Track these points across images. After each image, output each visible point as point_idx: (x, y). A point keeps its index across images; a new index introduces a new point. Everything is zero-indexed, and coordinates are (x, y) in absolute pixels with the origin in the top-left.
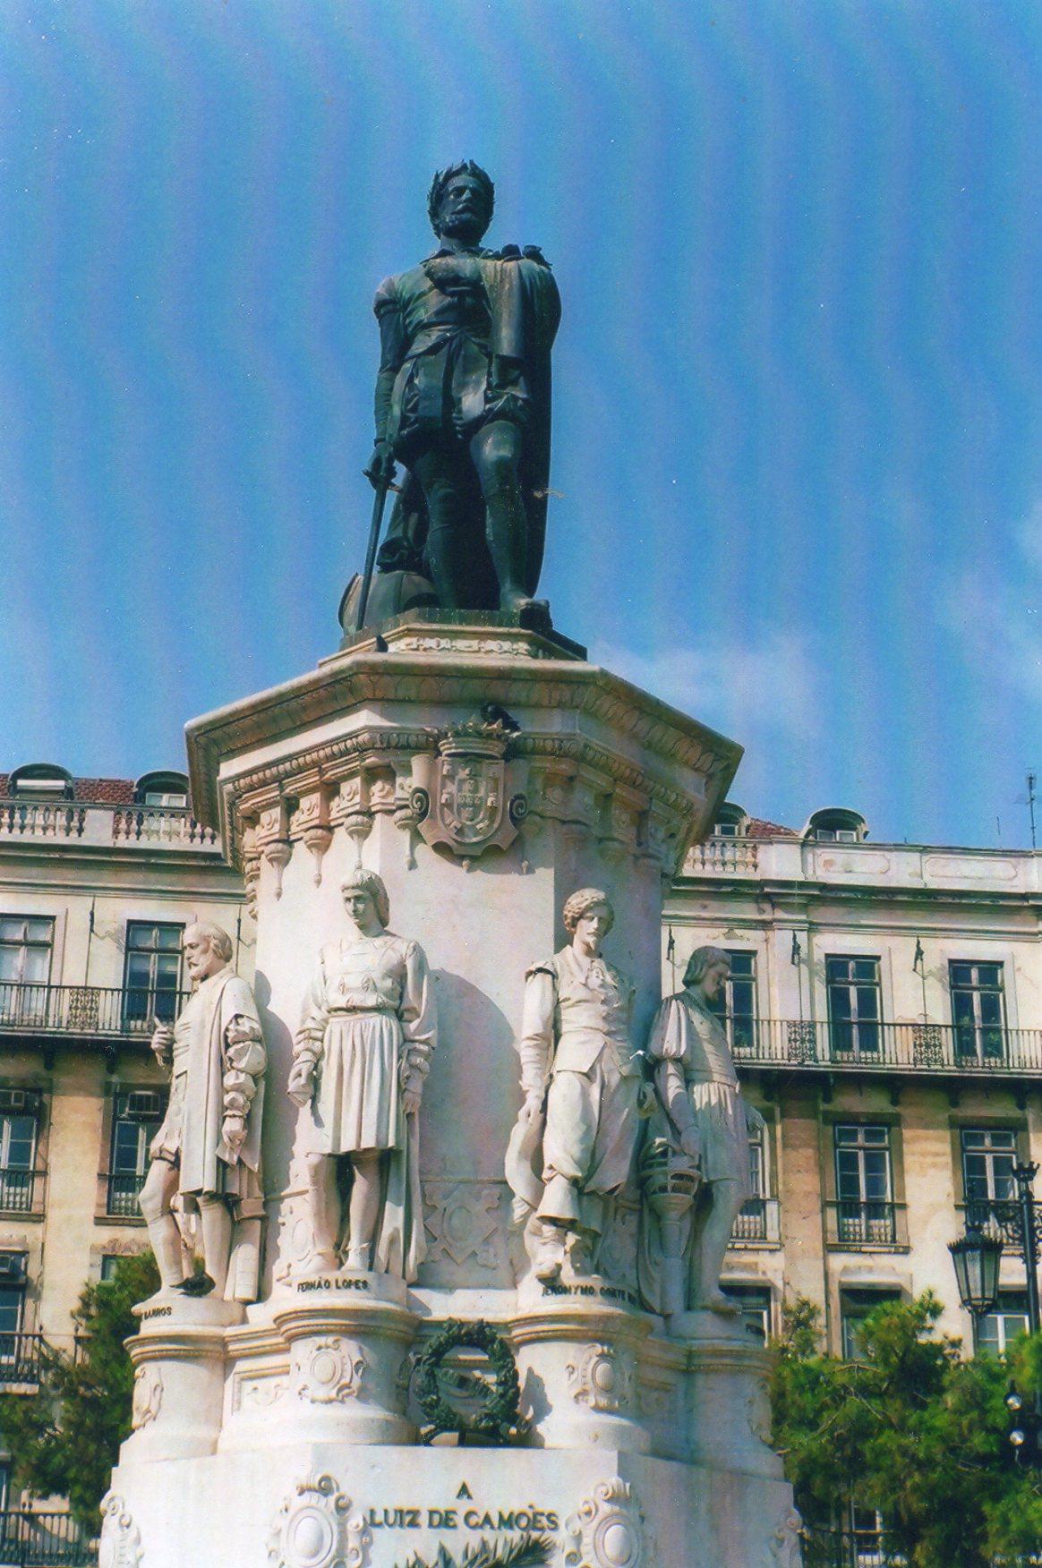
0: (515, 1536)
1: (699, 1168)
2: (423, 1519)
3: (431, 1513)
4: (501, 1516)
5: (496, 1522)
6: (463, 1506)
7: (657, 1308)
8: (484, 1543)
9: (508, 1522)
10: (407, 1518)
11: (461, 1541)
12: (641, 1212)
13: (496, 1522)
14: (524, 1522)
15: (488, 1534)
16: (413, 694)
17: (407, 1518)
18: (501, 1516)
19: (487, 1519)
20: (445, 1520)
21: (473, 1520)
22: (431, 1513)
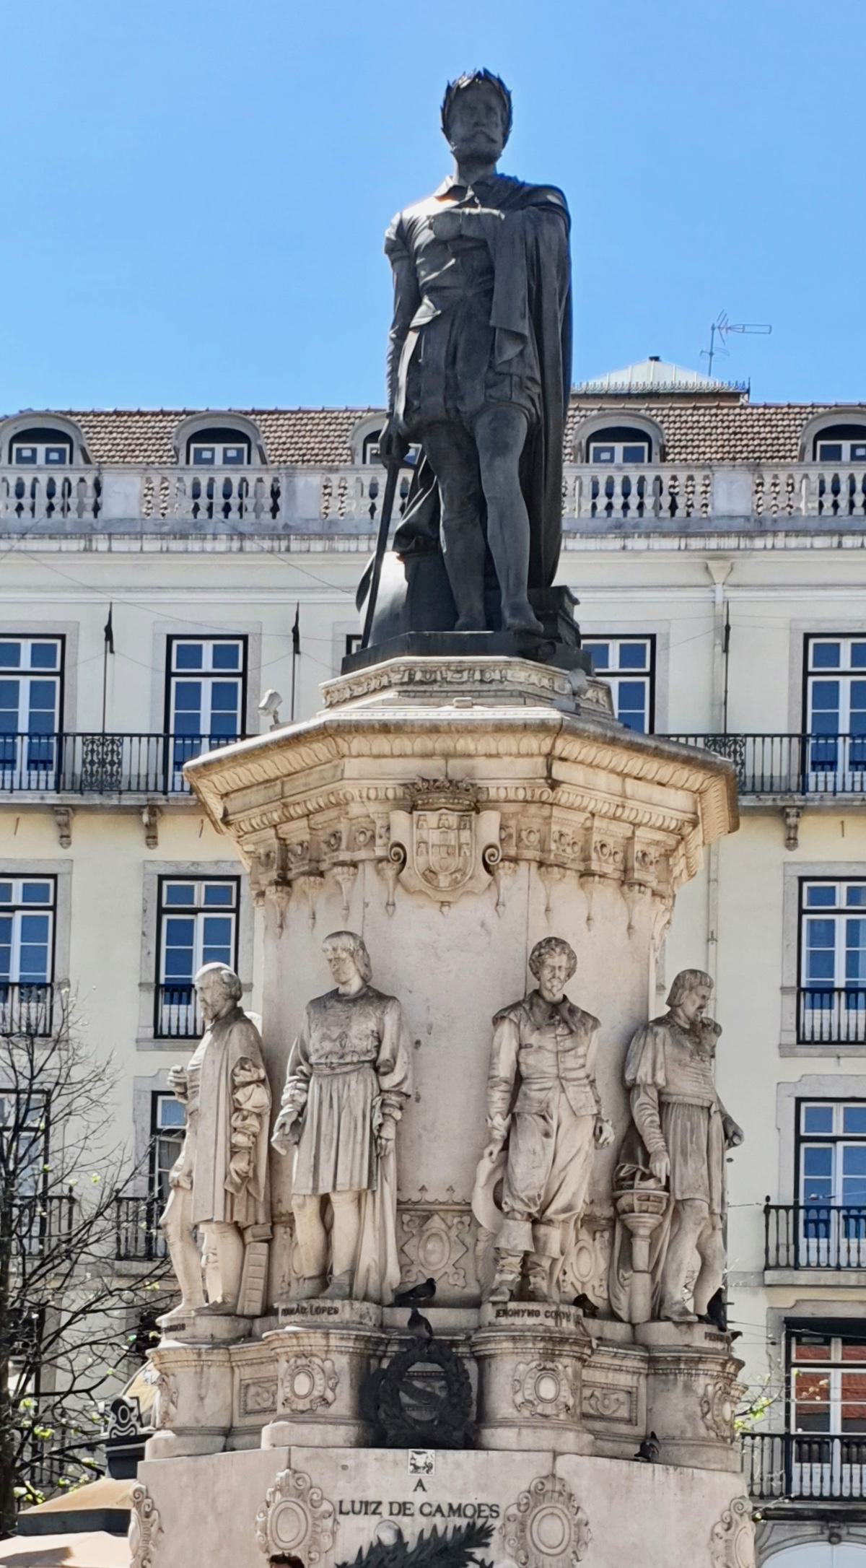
0: (462, 1522)
1: (667, 1188)
2: (384, 1509)
3: (391, 1504)
4: (450, 1506)
5: (445, 1509)
6: (419, 1498)
7: (625, 1317)
8: (435, 1528)
9: (457, 1511)
10: (370, 1508)
11: (413, 1528)
12: (614, 1228)
13: (445, 1509)
14: (469, 1512)
15: (438, 1520)
16: (387, 750)
17: (370, 1508)
18: (450, 1506)
19: (439, 1509)
20: (403, 1508)
21: (427, 1510)
22: (391, 1504)
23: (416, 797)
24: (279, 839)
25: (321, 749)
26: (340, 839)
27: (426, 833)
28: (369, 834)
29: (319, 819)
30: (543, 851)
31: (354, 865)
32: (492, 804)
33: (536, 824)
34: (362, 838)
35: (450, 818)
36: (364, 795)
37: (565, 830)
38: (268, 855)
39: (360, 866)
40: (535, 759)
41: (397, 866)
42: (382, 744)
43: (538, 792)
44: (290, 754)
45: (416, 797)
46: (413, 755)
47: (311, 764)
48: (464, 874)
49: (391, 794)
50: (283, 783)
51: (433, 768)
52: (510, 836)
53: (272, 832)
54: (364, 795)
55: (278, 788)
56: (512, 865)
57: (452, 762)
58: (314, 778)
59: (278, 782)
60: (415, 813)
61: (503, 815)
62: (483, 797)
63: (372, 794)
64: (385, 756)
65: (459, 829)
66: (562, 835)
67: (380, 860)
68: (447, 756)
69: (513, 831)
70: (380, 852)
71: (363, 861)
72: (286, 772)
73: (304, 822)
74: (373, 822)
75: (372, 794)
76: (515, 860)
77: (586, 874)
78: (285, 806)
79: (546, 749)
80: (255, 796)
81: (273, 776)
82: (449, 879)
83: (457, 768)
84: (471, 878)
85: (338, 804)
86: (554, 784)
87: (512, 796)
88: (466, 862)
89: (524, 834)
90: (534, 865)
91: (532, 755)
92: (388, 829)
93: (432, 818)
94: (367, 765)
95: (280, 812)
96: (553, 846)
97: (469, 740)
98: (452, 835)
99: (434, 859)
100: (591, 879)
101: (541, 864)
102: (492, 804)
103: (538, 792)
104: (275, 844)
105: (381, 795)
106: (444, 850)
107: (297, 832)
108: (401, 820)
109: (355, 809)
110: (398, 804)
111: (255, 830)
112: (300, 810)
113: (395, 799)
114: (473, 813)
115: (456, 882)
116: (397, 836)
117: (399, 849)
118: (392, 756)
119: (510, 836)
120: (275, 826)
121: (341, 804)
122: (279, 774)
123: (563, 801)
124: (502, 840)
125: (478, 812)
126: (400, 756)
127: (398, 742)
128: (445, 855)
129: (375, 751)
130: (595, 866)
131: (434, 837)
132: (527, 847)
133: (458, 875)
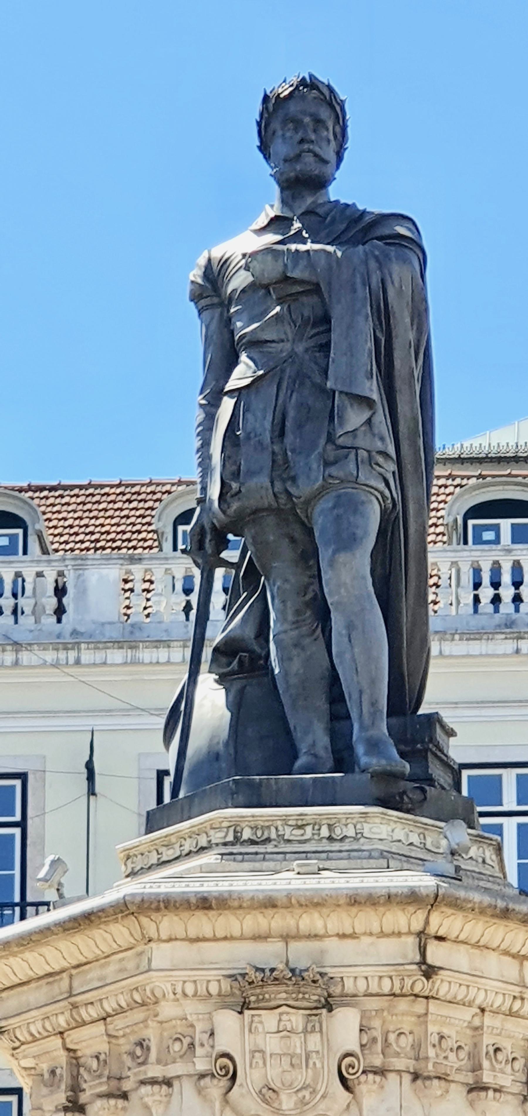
23: (247, 992)
24: (69, 1050)
25: (120, 932)
26: (148, 1049)
27: (260, 1040)
28: (186, 1041)
29: (118, 1023)
30: (417, 1059)
31: (168, 1083)
32: (349, 999)
33: (407, 1024)
34: (177, 1046)
35: (293, 1018)
36: (179, 990)
37: (446, 1031)
38: (53, 1072)
39: (176, 1084)
40: (403, 939)
41: (224, 1082)
42: (201, 923)
43: (408, 982)
44: (79, 939)
45: (247, 992)
46: (242, 938)
47: (107, 951)
48: (314, 1092)
49: (214, 989)
50: (71, 977)
51: (269, 954)
52: (374, 1040)
53: (57, 1041)
54: (179, 990)
55: (65, 984)
56: (378, 1078)
57: (295, 946)
58: (111, 971)
59: (64, 975)
60: (247, 1012)
61: (364, 1015)
62: (336, 990)
63: (190, 989)
64: (205, 940)
65: (305, 1031)
66: (442, 1037)
67: (202, 1076)
68: (286, 938)
69: (378, 1034)
70: (201, 1065)
71: (178, 1077)
72: (75, 963)
73: (100, 1027)
74: (192, 1026)
75: (190, 989)
76: (381, 1072)
77: (477, 1088)
78: (75, 1006)
79: (417, 925)
80: (33, 995)
81: (57, 968)
82: (294, 1098)
83: (300, 953)
84: (323, 1097)
85: (143, 1004)
86: (429, 972)
87: (374, 988)
88: (315, 1080)
89: (392, 1037)
90: (407, 1078)
91: (399, 934)
92: (212, 1034)
93: (269, 1020)
94: (182, 951)
95: (67, 1014)
96: (431, 1053)
97: (316, 915)
98: (297, 1041)
99: (274, 1073)
100: (483, 1094)
101: (416, 1076)
102: (349, 999)
103: (408, 982)
104: (62, 1057)
105: (202, 990)
106: (286, 1060)
107: (90, 1041)
108: (227, 1022)
109: (167, 1010)
110: (224, 1001)
111: (35, 1040)
112: (94, 1012)
113: (219, 995)
114: (324, 1011)
115: (303, 1102)
116: (222, 1044)
117: (225, 1061)
118: (215, 939)
119: (374, 1040)
120: (61, 1033)
121: (148, 1003)
122: (65, 965)
123: (441, 993)
124: (362, 1046)
125: (330, 1010)
126: (225, 938)
127: (221, 920)
128: (287, 1067)
129: (192, 933)
130: (487, 1078)
131: (273, 1044)
132: (397, 1055)
133: (306, 1093)
